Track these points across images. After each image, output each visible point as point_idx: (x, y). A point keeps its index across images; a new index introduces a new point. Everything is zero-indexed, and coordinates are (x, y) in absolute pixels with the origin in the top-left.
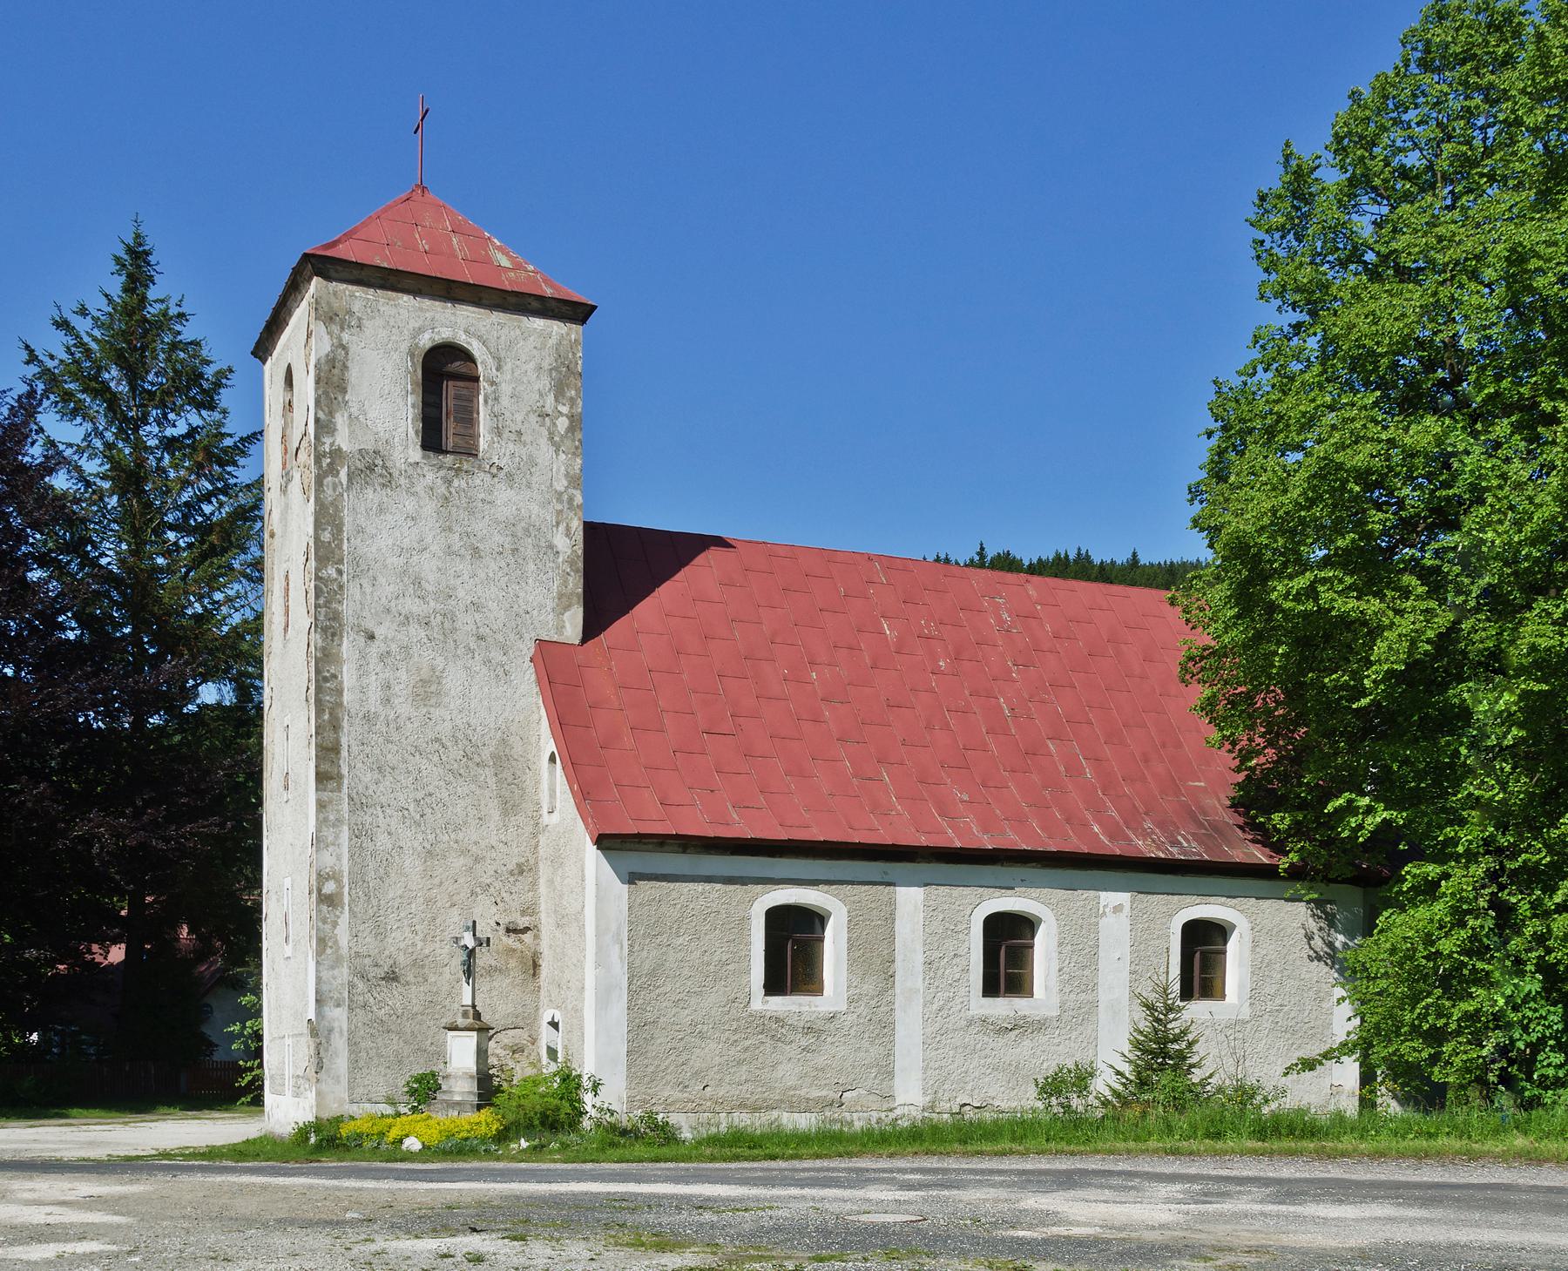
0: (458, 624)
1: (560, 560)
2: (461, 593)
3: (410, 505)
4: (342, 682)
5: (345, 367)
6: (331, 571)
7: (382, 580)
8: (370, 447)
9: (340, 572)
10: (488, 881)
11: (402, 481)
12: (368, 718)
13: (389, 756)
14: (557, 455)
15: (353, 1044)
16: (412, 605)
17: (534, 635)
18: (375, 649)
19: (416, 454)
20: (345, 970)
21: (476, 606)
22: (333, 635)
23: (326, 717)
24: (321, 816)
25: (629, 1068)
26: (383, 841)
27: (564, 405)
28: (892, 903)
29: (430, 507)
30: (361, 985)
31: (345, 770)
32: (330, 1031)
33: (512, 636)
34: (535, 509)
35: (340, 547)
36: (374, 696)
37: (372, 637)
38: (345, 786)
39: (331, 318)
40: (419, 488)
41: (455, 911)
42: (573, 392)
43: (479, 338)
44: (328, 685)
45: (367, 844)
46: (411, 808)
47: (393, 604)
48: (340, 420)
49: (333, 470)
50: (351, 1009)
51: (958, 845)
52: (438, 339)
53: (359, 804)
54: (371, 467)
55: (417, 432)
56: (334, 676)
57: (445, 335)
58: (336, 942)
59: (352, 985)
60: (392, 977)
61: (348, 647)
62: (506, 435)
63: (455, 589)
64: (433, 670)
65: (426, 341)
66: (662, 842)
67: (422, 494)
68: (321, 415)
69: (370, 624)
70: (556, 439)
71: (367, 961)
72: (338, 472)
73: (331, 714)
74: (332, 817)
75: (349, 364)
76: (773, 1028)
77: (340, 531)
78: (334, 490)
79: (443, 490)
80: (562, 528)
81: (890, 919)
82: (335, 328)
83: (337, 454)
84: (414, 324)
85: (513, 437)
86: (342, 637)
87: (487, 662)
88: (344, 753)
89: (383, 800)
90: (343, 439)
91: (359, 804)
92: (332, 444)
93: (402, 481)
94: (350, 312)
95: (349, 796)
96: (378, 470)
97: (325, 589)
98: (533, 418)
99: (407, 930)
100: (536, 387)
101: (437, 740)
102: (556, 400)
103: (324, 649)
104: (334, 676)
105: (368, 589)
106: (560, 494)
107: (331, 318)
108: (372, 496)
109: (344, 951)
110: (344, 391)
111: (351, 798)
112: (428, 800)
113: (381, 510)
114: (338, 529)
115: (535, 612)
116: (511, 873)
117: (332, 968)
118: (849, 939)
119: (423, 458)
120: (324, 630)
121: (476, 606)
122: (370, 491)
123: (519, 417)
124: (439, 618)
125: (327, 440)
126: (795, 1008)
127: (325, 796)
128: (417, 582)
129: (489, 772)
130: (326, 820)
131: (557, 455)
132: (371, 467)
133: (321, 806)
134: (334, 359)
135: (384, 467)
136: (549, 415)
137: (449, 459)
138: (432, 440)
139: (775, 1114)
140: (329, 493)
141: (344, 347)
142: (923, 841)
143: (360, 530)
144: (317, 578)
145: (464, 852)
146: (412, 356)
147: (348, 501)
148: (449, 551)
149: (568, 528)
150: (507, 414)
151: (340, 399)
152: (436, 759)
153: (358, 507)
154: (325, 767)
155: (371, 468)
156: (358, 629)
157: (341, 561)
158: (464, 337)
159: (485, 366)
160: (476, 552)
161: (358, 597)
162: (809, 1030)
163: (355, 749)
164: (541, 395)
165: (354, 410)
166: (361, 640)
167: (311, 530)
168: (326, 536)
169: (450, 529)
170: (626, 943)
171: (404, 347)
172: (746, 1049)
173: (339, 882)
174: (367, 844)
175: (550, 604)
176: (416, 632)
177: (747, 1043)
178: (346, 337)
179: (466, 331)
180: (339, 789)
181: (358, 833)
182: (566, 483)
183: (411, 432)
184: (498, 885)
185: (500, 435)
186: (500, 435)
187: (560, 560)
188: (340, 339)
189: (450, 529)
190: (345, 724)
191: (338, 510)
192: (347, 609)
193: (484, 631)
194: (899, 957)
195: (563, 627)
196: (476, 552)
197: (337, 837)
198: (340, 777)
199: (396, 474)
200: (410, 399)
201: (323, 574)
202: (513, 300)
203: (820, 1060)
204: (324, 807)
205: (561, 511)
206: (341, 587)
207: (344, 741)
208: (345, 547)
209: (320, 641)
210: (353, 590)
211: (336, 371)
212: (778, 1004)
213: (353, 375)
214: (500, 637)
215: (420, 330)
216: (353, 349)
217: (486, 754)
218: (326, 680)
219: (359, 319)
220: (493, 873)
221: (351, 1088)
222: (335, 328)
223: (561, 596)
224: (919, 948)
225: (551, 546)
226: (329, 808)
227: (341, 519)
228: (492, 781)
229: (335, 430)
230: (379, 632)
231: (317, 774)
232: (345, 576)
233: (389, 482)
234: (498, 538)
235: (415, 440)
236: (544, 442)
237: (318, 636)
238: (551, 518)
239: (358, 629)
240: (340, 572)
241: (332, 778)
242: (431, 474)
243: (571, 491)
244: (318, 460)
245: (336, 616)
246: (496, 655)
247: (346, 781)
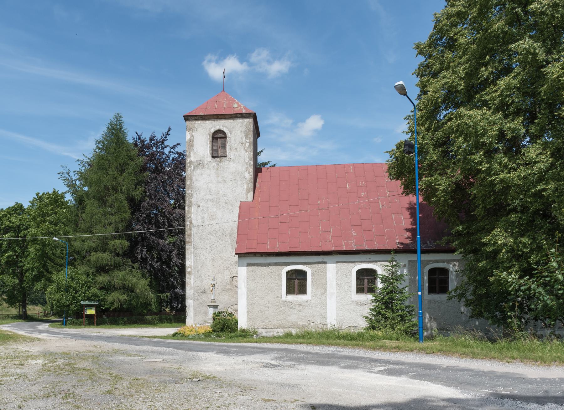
0: (220, 200)
2: (221, 192)
3: (208, 172)
5: (193, 141)
7: (201, 191)
8: (199, 159)
11: (207, 166)
15: (195, 309)
16: (208, 197)
17: (240, 201)
18: (201, 208)
19: (210, 158)
20: (193, 291)
21: (225, 195)
25: (247, 316)
26: (202, 257)
28: (326, 268)
29: (213, 172)
30: (197, 294)
31: (193, 240)
32: (189, 306)
34: (240, 168)
35: (191, 185)
36: (200, 221)
37: (199, 206)
40: (211, 167)
41: (220, 274)
45: (198, 258)
46: (209, 248)
50: (194, 300)
51: (344, 249)
52: (216, 129)
56: (190, 217)
58: (191, 284)
59: (194, 294)
60: (204, 292)
62: (233, 150)
65: (213, 131)
66: (255, 254)
69: (199, 203)
71: (198, 288)
76: (287, 304)
77: (192, 181)
79: (216, 167)
80: (247, 172)
81: (325, 272)
82: (191, 132)
84: (209, 127)
87: (227, 209)
88: (192, 236)
89: (202, 247)
93: (207, 166)
94: (194, 127)
96: (201, 164)
99: (208, 280)
101: (215, 230)
102: (246, 139)
104: (190, 217)
105: (198, 194)
108: (199, 171)
109: (193, 286)
110: (193, 147)
111: (194, 247)
112: (213, 246)
113: (201, 174)
117: (190, 290)
118: (312, 279)
121: (225, 195)
122: (199, 170)
124: (215, 199)
126: (296, 299)
128: (210, 191)
129: (228, 237)
135: (202, 164)
137: (218, 159)
139: (290, 329)
141: (193, 136)
142: (333, 249)
143: (197, 180)
145: (222, 259)
146: (209, 135)
147: (194, 173)
148: (218, 182)
155: (199, 164)
156: (196, 204)
157: (192, 188)
159: (228, 134)
162: (300, 305)
163: (195, 235)
166: (196, 207)
170: (246, 282)
171: (207, 133)
172: (281, 311)
173: (191, 268)
174: (198, 258)
176: (210, 204)
177: (281, 309)
178: (193, 134)
180: (191, 244)
183: (209, 153)
184: (231, 267)
185: (231, 150)
186: (231, 150)
189: (218, 176)
190: (193, 229)
191: (191, 176)
193: (227, 201)
194: (328, 283)
196: (225, 181)
197: (191, 257)
199: (205, 164)
202: (234, 116)
203: (303, 314)
206: (192, 195)
207: (192, 233)
210: (195, 195)
211: (191, 142)
212: (291, 298)
213: (195, 143)
214: (231, 202)
216: (195, 136)
217: (227, 233)
221: (194, 320)
223: (247, 189)
224: (335, 280)
228: (229, 240)
230: (201, 205)
233: (203, 167)
235: (210, 156)
238: (244, 169)
239: (196, 204)
240: (192, 191)
242: (214, 163)
243: (250, 162)
246: (230, 207)
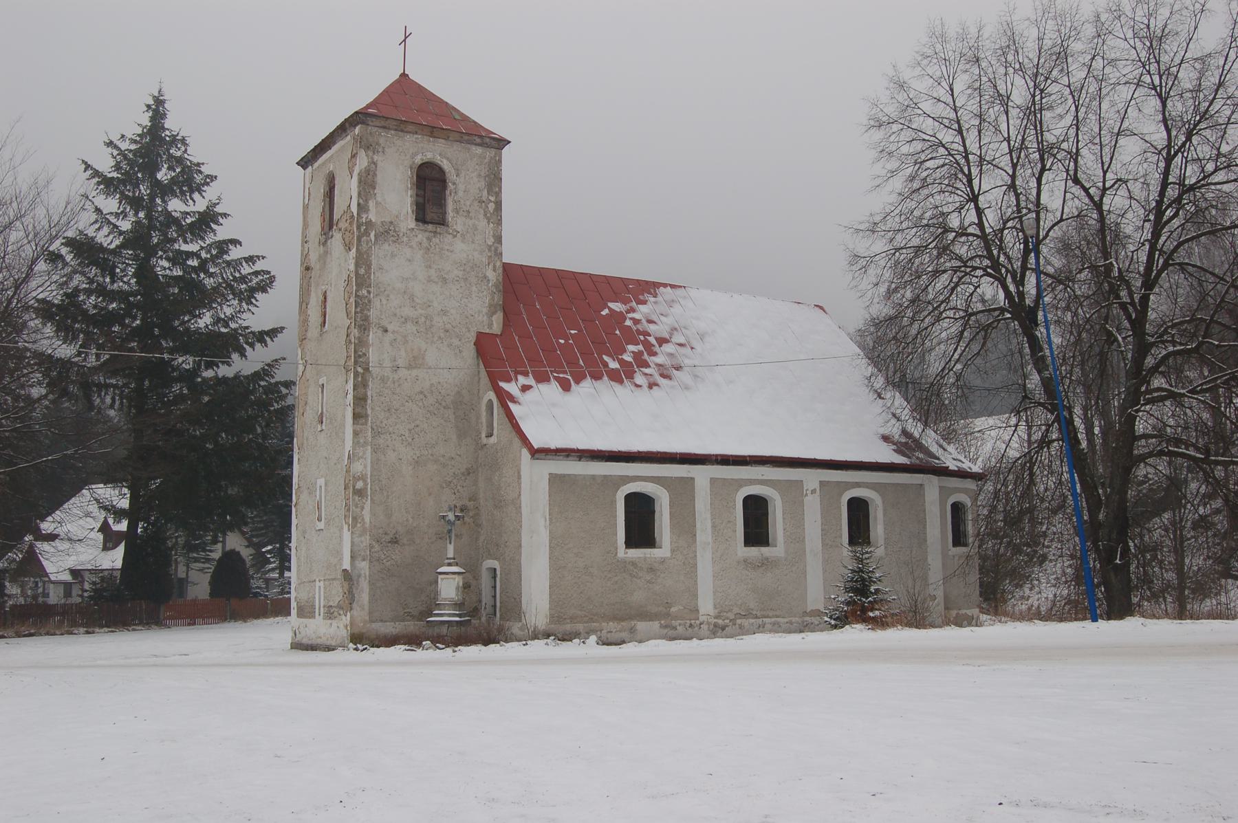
1: (490, 285)
2: (435, 304)
4: (369, 358)
6: (364, 292)
7: (392, 297)
8: (388, 219)
9: (369, 292)
10: (449, 480)
12: (383, 380)
13: (395, 402)
14: (489, 224)
18: (390, 336)
19: (412, 223)
22: (365, 329)
23: (360, 379)
24: (356, 440)
27: (492, 196)
31: (369, 412)
33: (464, 330)
37: (386, 331)
38: (369, 422)
39: (368, 147)
40: (414, 244)
42: (497, 189)
43: (448, 159)
44: (361, 360)
47: (398, 310)
48: (371, 204)
49: (367, 233)
53: (377, 433)
54: (388, 232)
55: (413, 211)
56: (365, 354)
57: (429, 156)
61: (372, 337)
63: (432, 302)
64: (420, 350)
65: (419, 160)
67: (415, 246)
68: (361, 201)
69: (385, 323)
70: (488, 215)
72: (370, 234)
73: (362, 377)
74: (361, 441)
75: (377, 173)
77: (370, 268)
78: (367, 244)
82: (370, 153)
83: (369, 224)
85: (465, 214)
86: (369, 330)
87: (450, 345)
88: (369, 401)
90: (372, 216)
91: (377, 433)
92: (367, 218)
93: (405, 239)
94: (378, 144)
95: (371, 428)
97: (361, 303)
98: (476, 204)
100: (477, 187)
101: (421, 392)
103: (359, 338)
105: (384, 302)
106: (490, 246)
107: (368, 147)
112: (417, 429)
113: (393, 256)
114: (369, 267)
115: (476, 316)
116: (463, 474)
119: (416, 225)
120: (360, 326)
121: (444, 312)
123: (468, 203)
125: (364, 216)
127: (358, 427)
128: (412, 298)
130: (358, 442)
131: (489, 224)
132: (388, 232)
133: (356, 434)
134: (369, 171)
135: (395, 231)
136: (484, 202)
137: (430, 227)
138: (421, 217)
140: (364, 247)
141: (375, 163)
144: (357, 296)
148: (429, 280)
149: (494, 266)
150: (462, 202)
151: (372, 192)
152: (421, 404)
153: (380, 254)
154: (358, 410)
157: (370, 286)
158: (439, 158)
160: (445, 281)
161: (379, 306)
163: (375, 398)
164: (480, 191)
165: (379, 199)
166: (380, 332)
167: (352, 267)
168: (362, 271)
169: (430, 267)
175: (485, 310)
176: (411, 327)
178: (376, 157)
179: (440, 155)
181: (375, 451)
182: (493, 241)
183: (410, 211)
187: (490, 285)
188: (372, 158)
189: (430, 267)
191: (369, 256)
192: (373, 314)
193: (449, 326)
195: (492, 324)
198: (367, 416)
200: (409, 193)
201: (360, 293)
204: (358, 435)
205: (491, 256)
206: (370, 301)
207: (369, 394)
208: (372, 277)
209: (357, 333)
210: (376, 303)
211: (369, 177)
213: (379, 178)
215: (416, 154)
216: (379, 164)
218: (360, 356)
219: (383, 148)
220: (452, 474)
222: (370, 153)
225: (485, 277)
226: (360, 435)
227: (371, 261)
229: (369, 210)
230: (390, 328)
231: (354, 414)
232: (372, 295)
234: (456, 272)
236: (481, 216)
237: (356, 330)
240: (369, 292)
241: (362, 417)
244: (359, 228)
245: (366, 318)
246: (456, 342)
247: (370, 419)
